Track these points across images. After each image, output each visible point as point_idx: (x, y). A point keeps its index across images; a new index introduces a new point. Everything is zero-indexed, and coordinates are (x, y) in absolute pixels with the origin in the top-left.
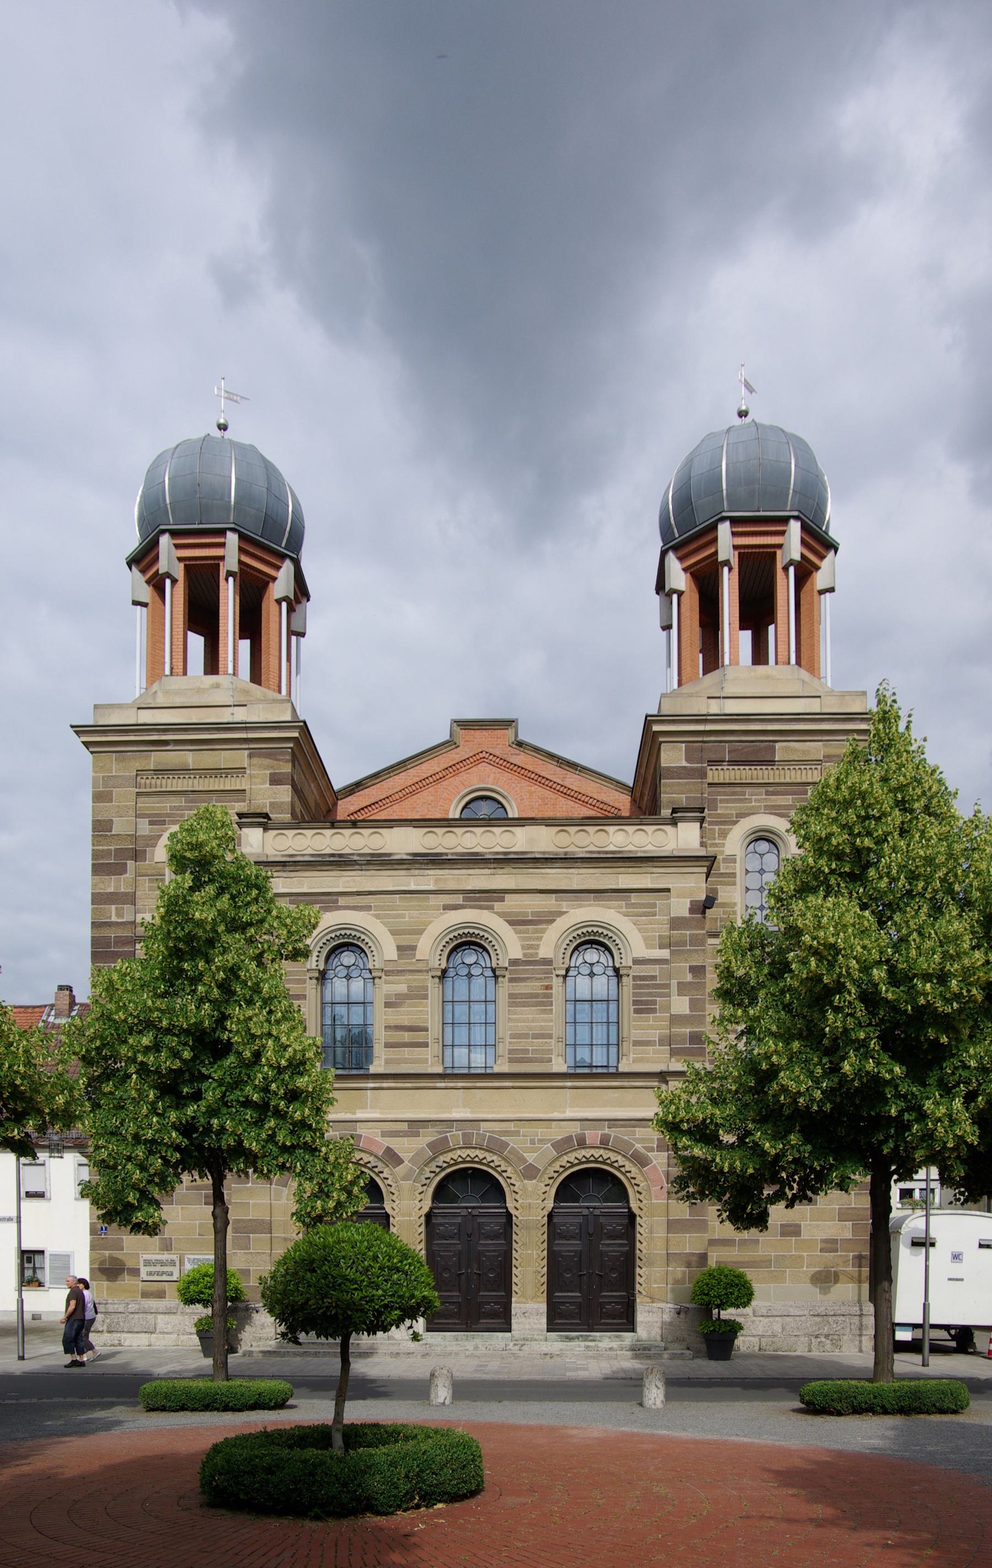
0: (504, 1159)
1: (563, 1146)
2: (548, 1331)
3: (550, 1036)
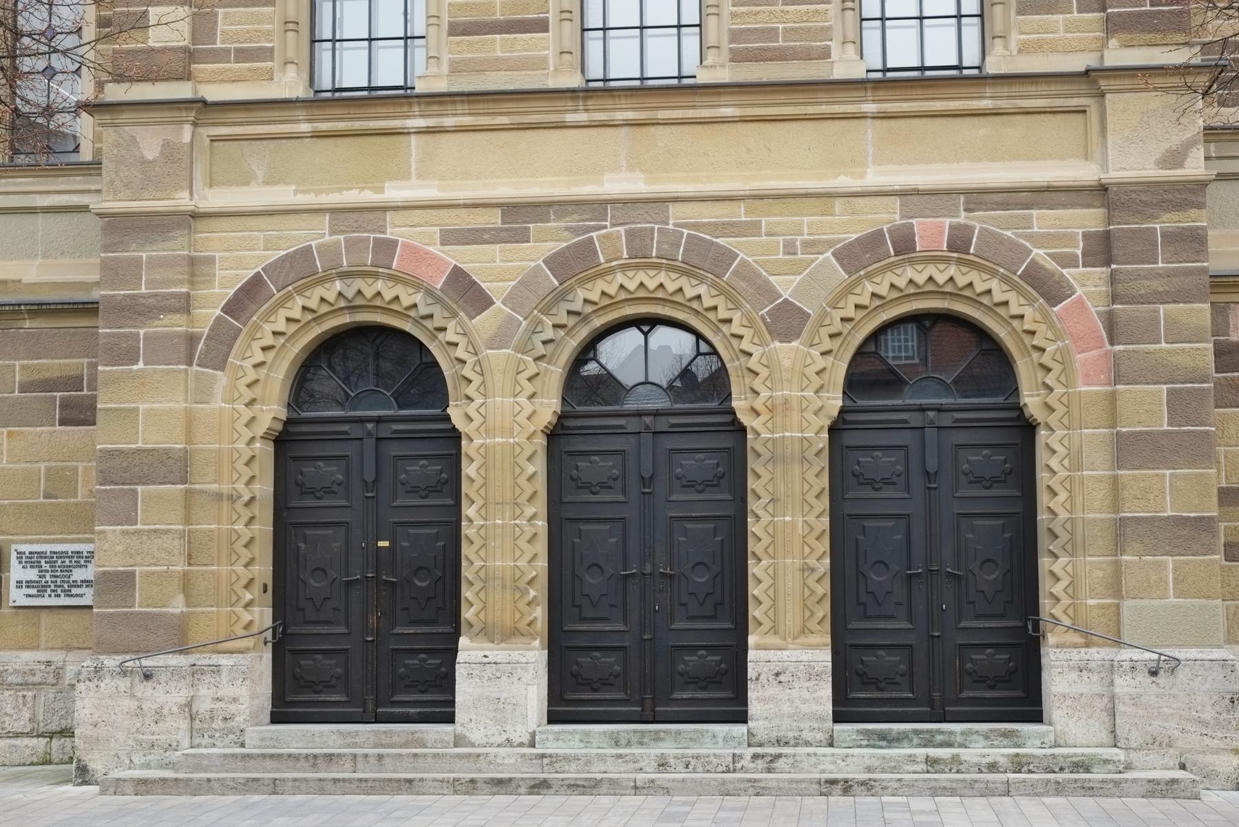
0: (722, 292)
1: (860, 255)
2: (838, 718)
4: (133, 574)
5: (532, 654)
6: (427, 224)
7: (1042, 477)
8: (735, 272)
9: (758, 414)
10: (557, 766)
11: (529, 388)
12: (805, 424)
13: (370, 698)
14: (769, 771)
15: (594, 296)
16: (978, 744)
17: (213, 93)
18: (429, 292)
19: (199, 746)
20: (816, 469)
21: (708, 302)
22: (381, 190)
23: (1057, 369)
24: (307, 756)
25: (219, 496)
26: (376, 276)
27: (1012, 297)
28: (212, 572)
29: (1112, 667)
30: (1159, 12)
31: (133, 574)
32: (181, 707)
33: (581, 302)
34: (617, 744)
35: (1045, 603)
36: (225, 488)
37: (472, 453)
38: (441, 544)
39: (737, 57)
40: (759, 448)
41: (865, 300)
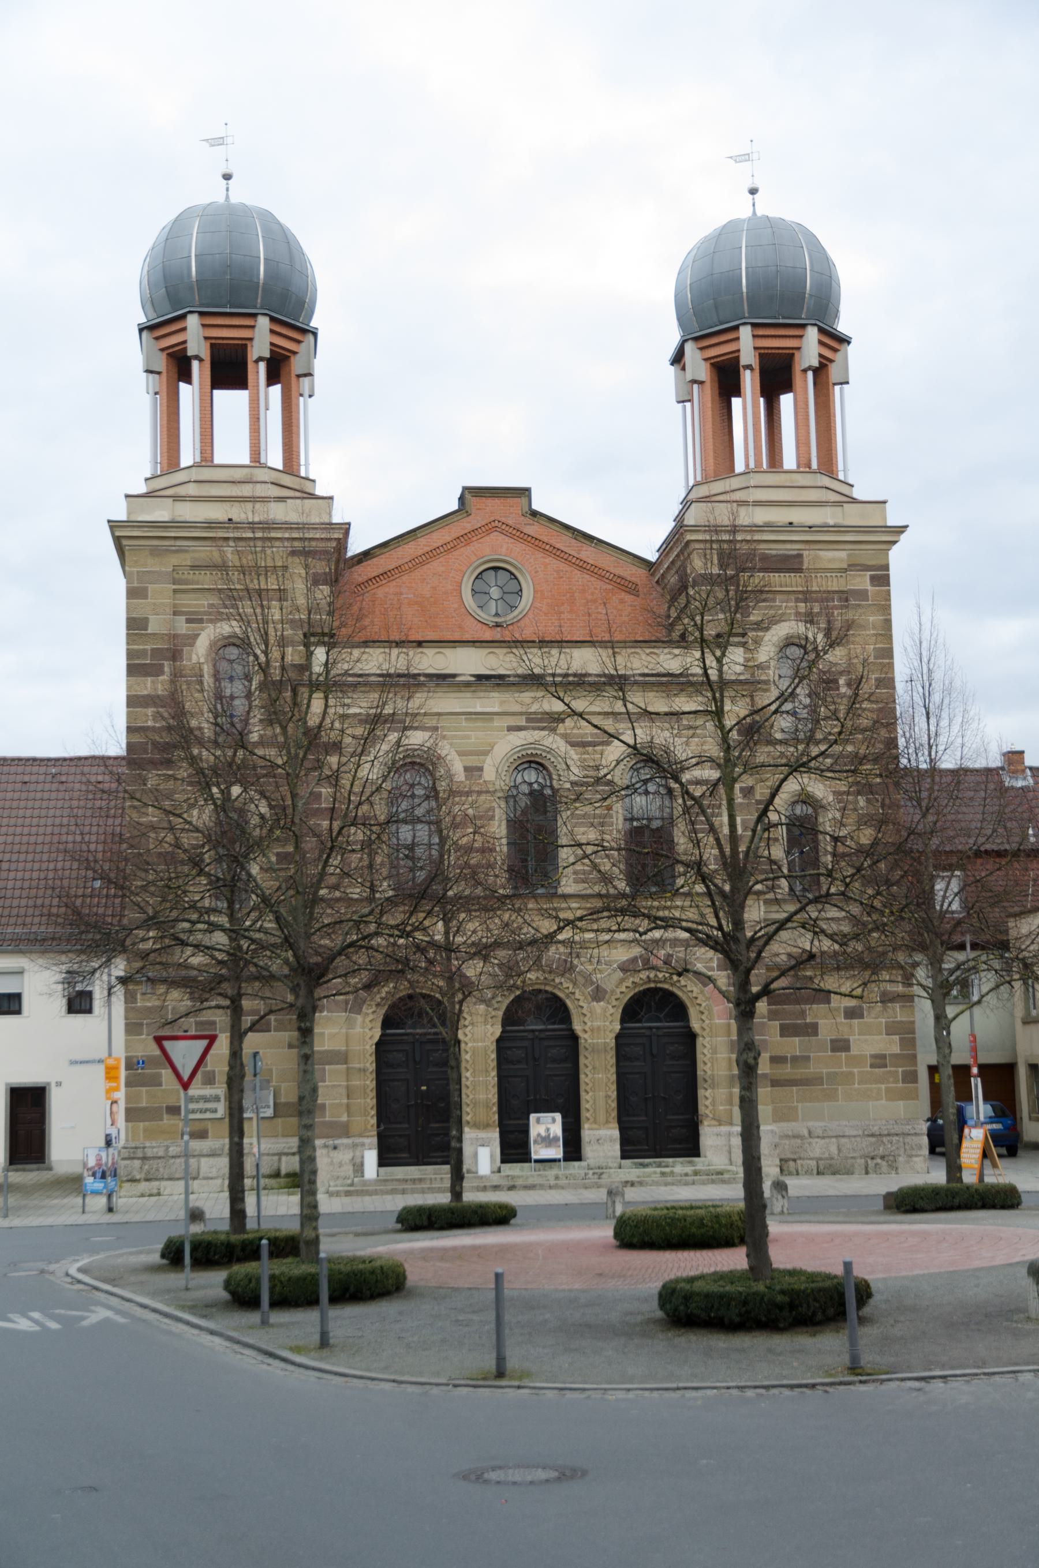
2: (623, 1157)
16: (679, 1166)
23: (706, 1012)
25: (360, 1069)
36: (362, 1066)
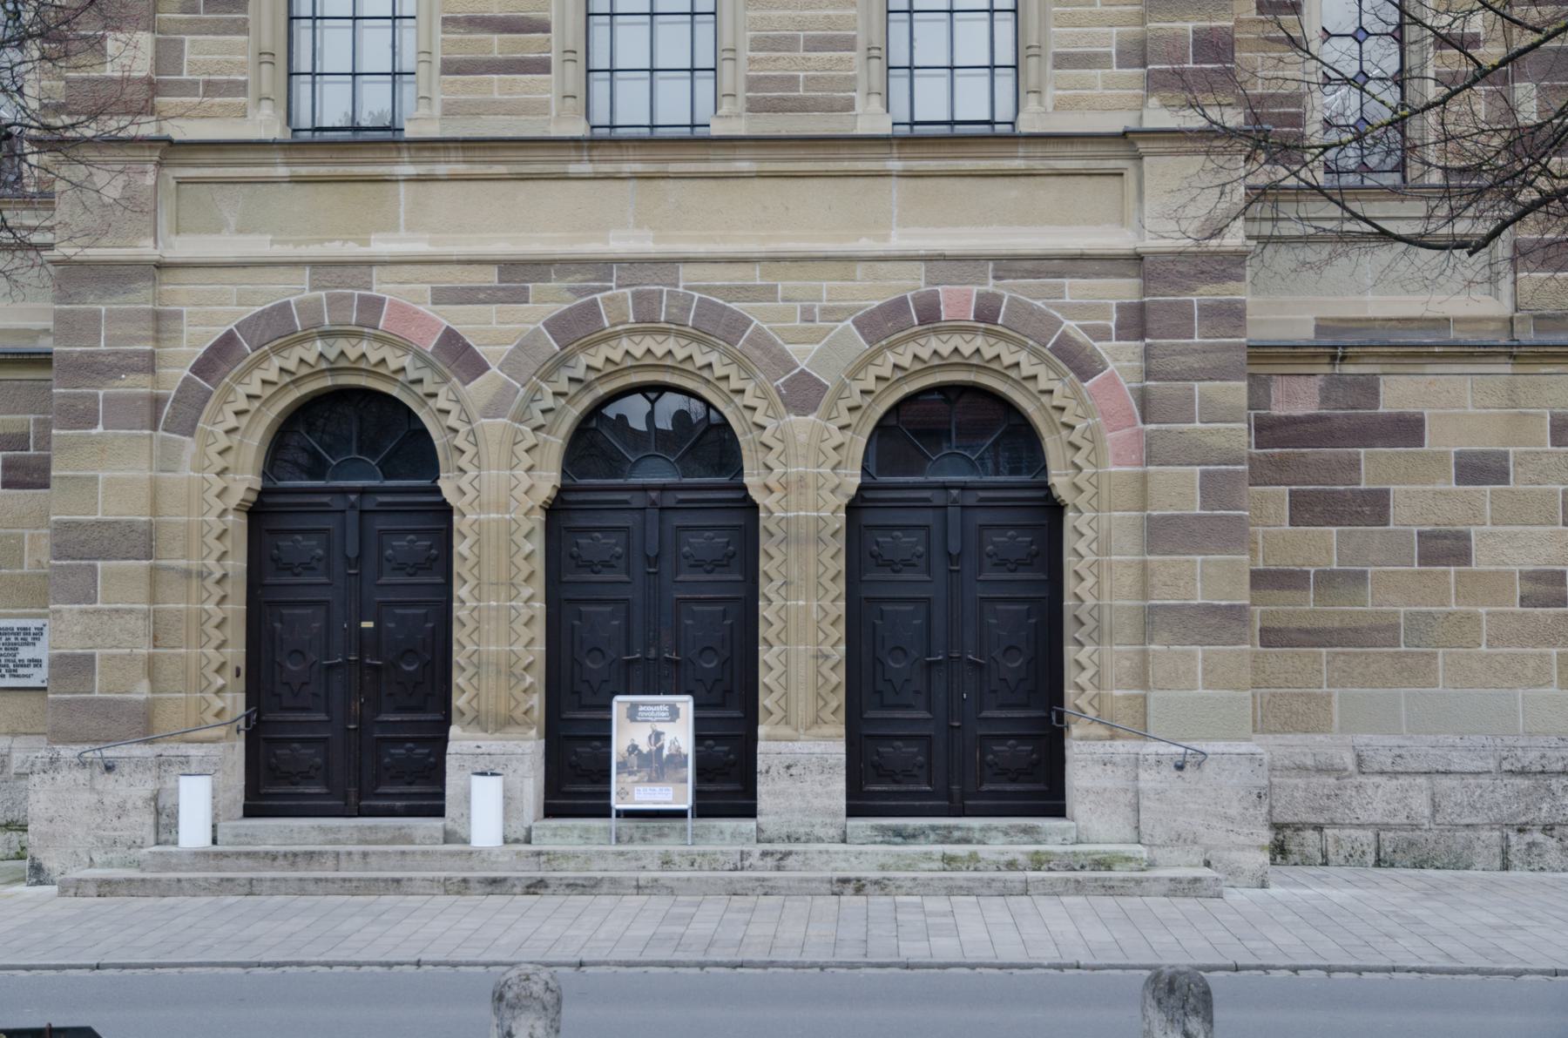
0: (734, 360)
1: (881, 325)
2: (852, 812)
3: (849, 44)
4: (92, 657)
5: (528, 744)
6: (417, 281)
7: (1069, 560)
8: (749, 340)
9: (771, 491)
10: (555, 864)
11: (527, 460)
12: (821, 503)
13: (353, 790)
14: (779, 869)
15: (598, 362)
16: (997, 839)
17: (182, 130)
18: (419, 355)
19: (166, 843)
20: (832, 550)
21: (719, 371)
22: (366, 243)
23: (1086, 447)
24: (285, 855)
25: (187, 574)
26: (360, 336)
27: (1040, 370)
28: (179, 655)
29: (1137, 761)
30: (1202, 70)
31: (90, 659)
32: (146, 801)
33: (583, 369)
34: (618, 840)
35: (1069, 692)
36: (194, 564)
37: (465, 529)
38: (430, 625)
39: (755, 107)
40: (772, 527)
41: (886, 371)
